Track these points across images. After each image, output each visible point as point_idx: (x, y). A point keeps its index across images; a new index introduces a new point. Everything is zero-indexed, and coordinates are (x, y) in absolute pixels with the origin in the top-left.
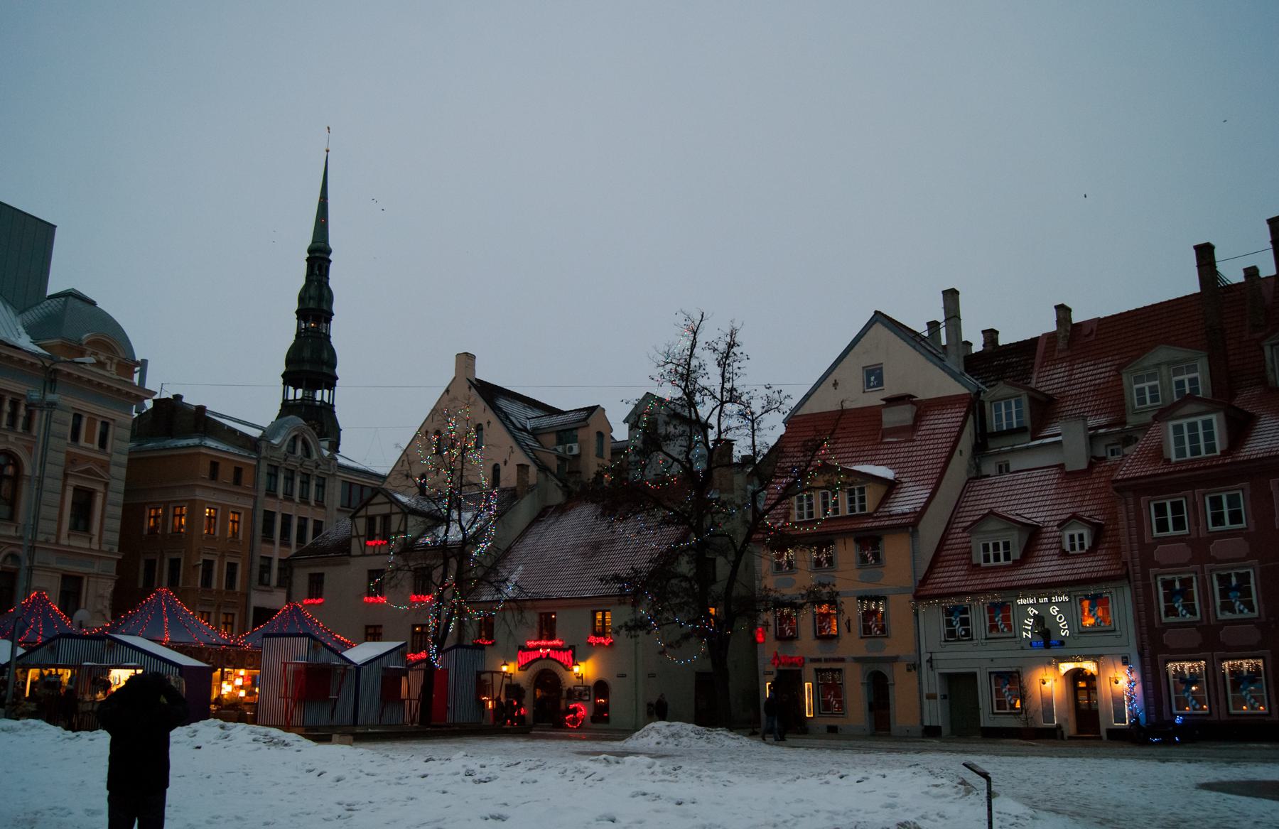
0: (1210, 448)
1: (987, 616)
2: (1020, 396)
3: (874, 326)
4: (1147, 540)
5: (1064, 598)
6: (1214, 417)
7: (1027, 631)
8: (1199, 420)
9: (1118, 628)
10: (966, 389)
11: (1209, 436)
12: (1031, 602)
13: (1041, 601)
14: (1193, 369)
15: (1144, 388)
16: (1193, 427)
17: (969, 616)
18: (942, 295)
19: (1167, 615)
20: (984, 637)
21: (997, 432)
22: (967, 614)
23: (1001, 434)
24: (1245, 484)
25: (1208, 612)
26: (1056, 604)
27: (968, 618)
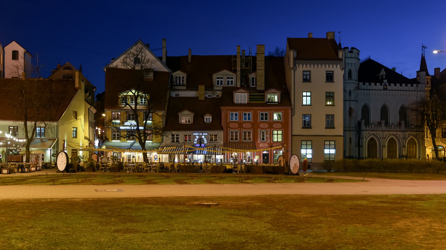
4: (228, 121)
5: (207, 134)
6: (246, 94)
7: (195, 142)
12: (197, 134)
13: (200, 134)
14: (232, 78)
15: (219, 81)
17: (179, 137)
19: (231, 140)
25: (241, 140)
26: (204, 135)
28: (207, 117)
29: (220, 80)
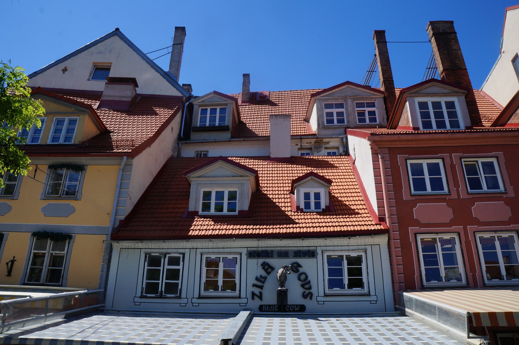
0: (455, 124)
1: (204, 269)
2: (226, 105)
3: (112, 38)
8: (443, 100)
9: (372, 292)
10: (180, 93)
11: (452, 115)
15: (332, 113)
16: (437, 105)
17: (180, 267)
18: (174, 30)
20: (196, 295)
21: (200, 127)
22: (178, 264)
23: (203, 129)
24: (500, 153)
27: (179, 270)
28: (307, 190)
29: (335, 111)
